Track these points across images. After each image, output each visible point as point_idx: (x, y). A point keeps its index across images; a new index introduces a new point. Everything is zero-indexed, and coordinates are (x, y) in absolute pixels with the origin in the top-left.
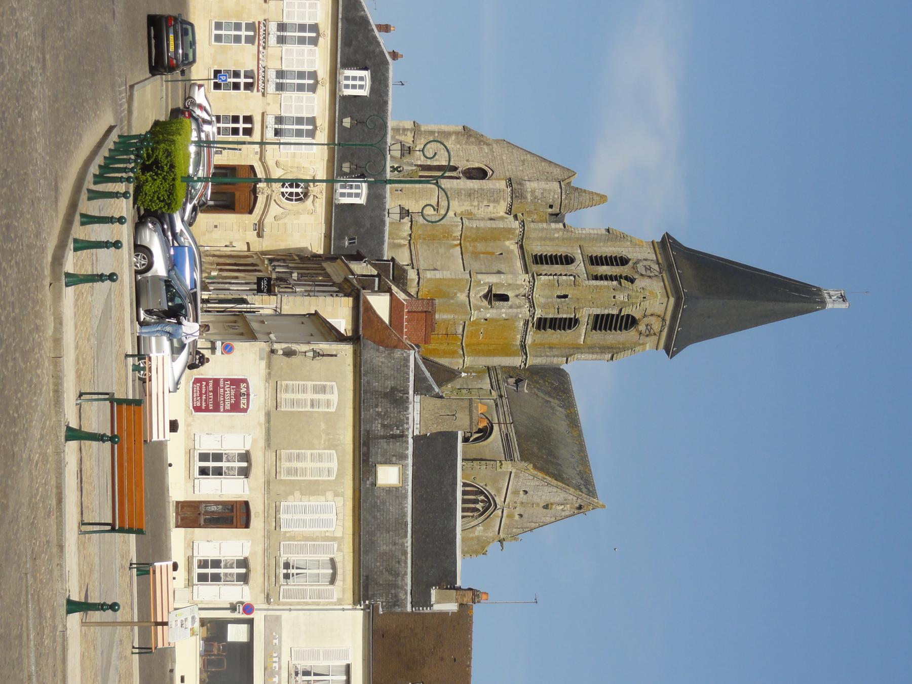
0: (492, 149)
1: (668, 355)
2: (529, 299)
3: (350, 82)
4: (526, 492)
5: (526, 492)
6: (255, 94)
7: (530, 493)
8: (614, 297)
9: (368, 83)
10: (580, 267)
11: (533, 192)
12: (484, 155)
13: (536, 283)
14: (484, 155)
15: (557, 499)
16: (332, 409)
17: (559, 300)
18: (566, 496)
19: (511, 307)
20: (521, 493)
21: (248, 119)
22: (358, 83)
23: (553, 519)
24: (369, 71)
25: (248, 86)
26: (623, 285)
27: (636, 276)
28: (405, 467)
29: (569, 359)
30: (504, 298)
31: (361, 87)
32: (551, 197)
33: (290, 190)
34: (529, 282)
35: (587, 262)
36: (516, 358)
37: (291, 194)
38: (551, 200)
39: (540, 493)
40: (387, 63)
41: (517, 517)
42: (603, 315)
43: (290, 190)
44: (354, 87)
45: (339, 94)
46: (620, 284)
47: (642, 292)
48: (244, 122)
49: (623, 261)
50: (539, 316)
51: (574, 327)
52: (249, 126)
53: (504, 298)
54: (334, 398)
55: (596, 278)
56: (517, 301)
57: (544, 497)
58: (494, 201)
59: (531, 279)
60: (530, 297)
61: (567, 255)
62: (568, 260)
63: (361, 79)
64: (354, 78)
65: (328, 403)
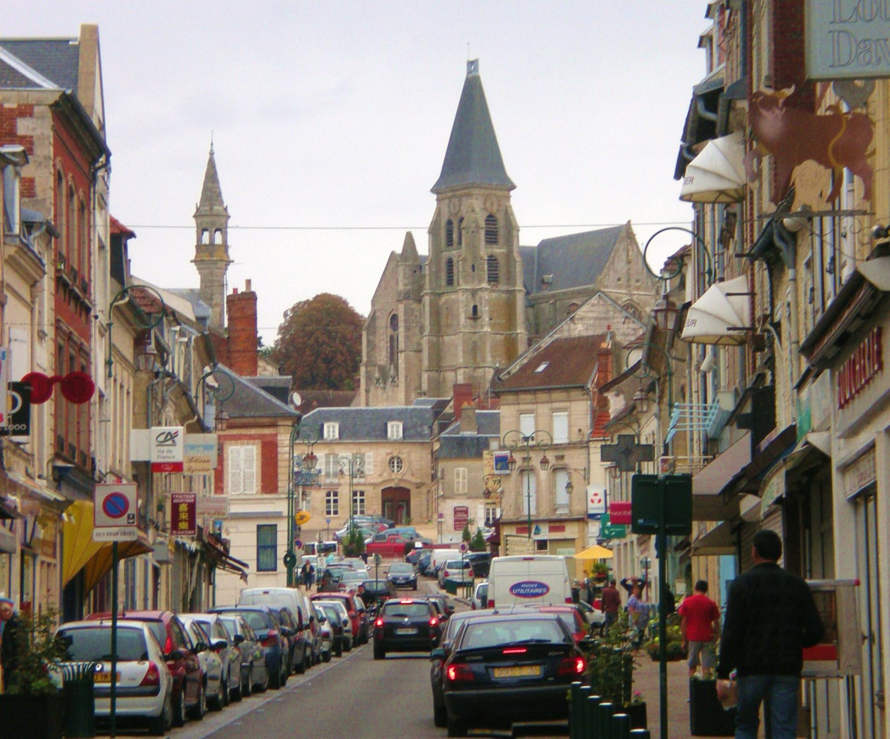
4: (619, 280)
5: (619, 280)
6: (339, 490)
7: (619, 276)
10: (454, 253)
11: (405, 285)
15: (624, 257)
16: (466, 470)
17: (476, 271)
18: (621, 250)
19: (481, 304)
20: (619, 282)
21: (355, 494)
22: (331, 430)
25: (336, 494)
27: (459, 216)
28: (491, 437)
30: (475, 308)
33: (396, 468)
35: (450, 248)
37: (398, 467)
41: (638, 284)
43: (396, 468)
44: (334, 432)
45: (337, 441)
48: (356, 495)
49: (450, 223)
52: (358, 494)
53: (475, 308)
54: (461, 469)
55: (460, 243)
56: (478, 299)
58: (413, 312)
62: (450, 262)
63: (329, 427)
65: (464, 472)
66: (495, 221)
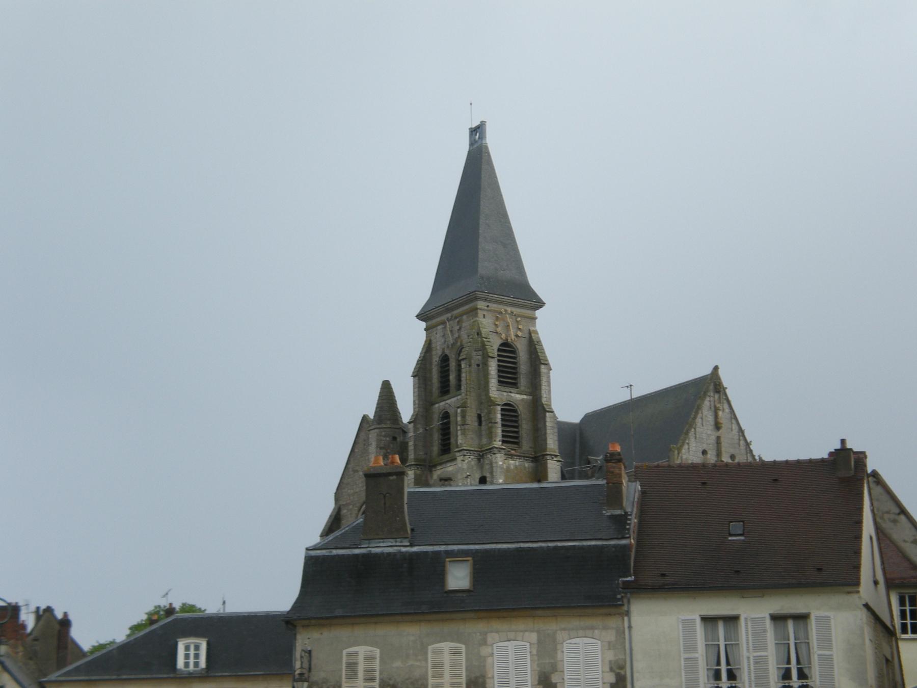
0: (343, 505)
1: (543, 306)
2: (483, 454)
3: (192, 661)
7: (705, 447)
8: (478, 365)
9: (192, 641)
12: (349, 513)
13: (465, 448)
14: (349, 513)
15: (710, 418)
16: (377, 652)
17: (484, 423)
22: (192, 652)
23: (734, 421)
24: (178, 640)
26: (464, 357)
28: (449, 554)
29: (548, 410)
31: (197, 648)
32: (384, 439)
34: (464, 455)
36: (549, 466)
38: (388, 439)
39: (704, 436)
40: (176, 620)
42: (499, 376)
44: (197, 656)
46: (463, 359)
47: (471, 337)
49: (445, 359)
50: (500, 443)
51: (515, 407)
54: (362, 651)
55: (459, 387)
57: (709, 432)
59: (461, 453)
60: (481, 454)
61: (442, 418)
62: (446, 416)
63: (187, 648)
64: (187, 656)
65: (369, 658)
66: (514, 352)
